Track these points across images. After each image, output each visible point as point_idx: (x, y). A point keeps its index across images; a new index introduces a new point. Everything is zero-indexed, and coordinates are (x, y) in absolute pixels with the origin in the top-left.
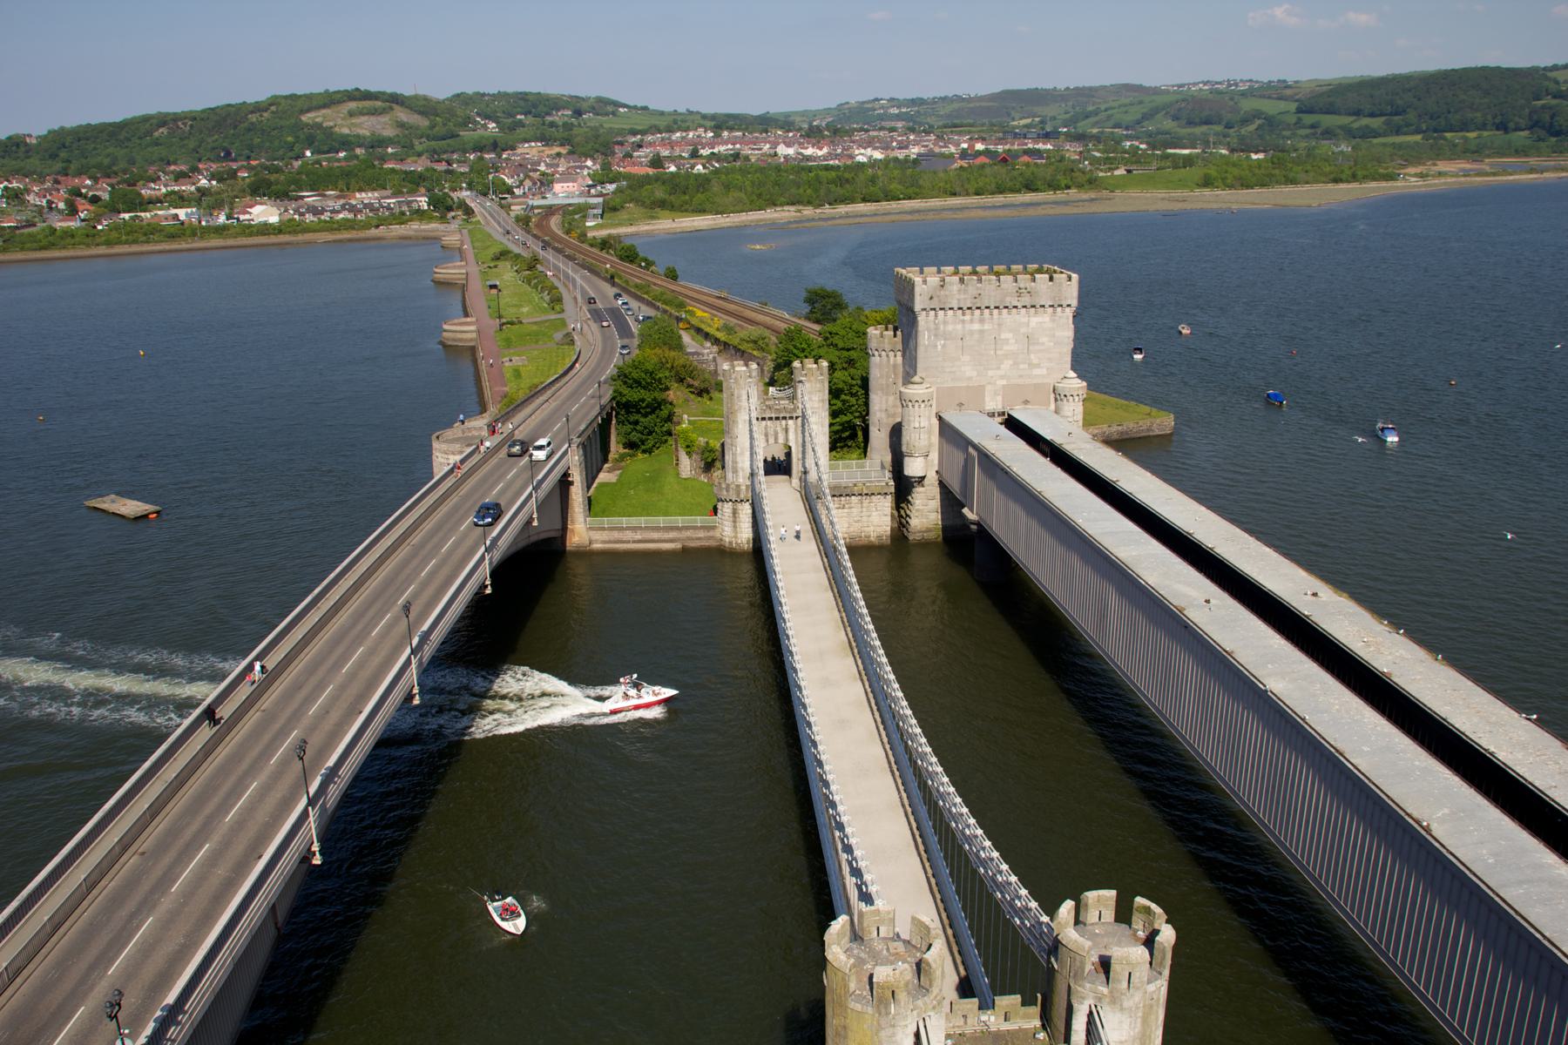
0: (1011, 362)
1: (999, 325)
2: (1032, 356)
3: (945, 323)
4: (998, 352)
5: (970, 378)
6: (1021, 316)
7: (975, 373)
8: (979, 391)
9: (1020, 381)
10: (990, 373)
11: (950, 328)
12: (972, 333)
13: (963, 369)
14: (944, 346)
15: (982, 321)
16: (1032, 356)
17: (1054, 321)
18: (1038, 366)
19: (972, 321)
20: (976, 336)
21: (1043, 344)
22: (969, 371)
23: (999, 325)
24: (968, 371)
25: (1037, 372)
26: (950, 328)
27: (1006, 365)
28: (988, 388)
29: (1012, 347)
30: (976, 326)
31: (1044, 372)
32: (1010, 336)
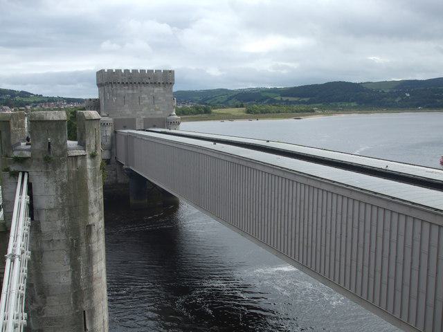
0: (146, 108)
1: (141, 91)
2: (156, 105)
3: (117, 89)
4: (141, 103)
5: (129, 115)
6: (150, 88)
7: (130, 113)
8: (134, 120)
9: (150, 116)
10: (138, 113)
11: (119, 92)
12: (128, 94)
13: (126, 110)
14: (116, 100)
15: (133, 89)
16: (156, 105)
17: (164, 90)
18: (158, 110)
19: (128, 89)
20: (131, 96)
21: (160, 100)
22: (128, 112)
23: (141, 91)
24: (127, 112)
25: (158, 112)
26: (119, 92)
27: (145, 109)
28: (137, 119)
29: (147, 101)
30: (130, 92)
31: (162, 112)
32: (145, 96)
